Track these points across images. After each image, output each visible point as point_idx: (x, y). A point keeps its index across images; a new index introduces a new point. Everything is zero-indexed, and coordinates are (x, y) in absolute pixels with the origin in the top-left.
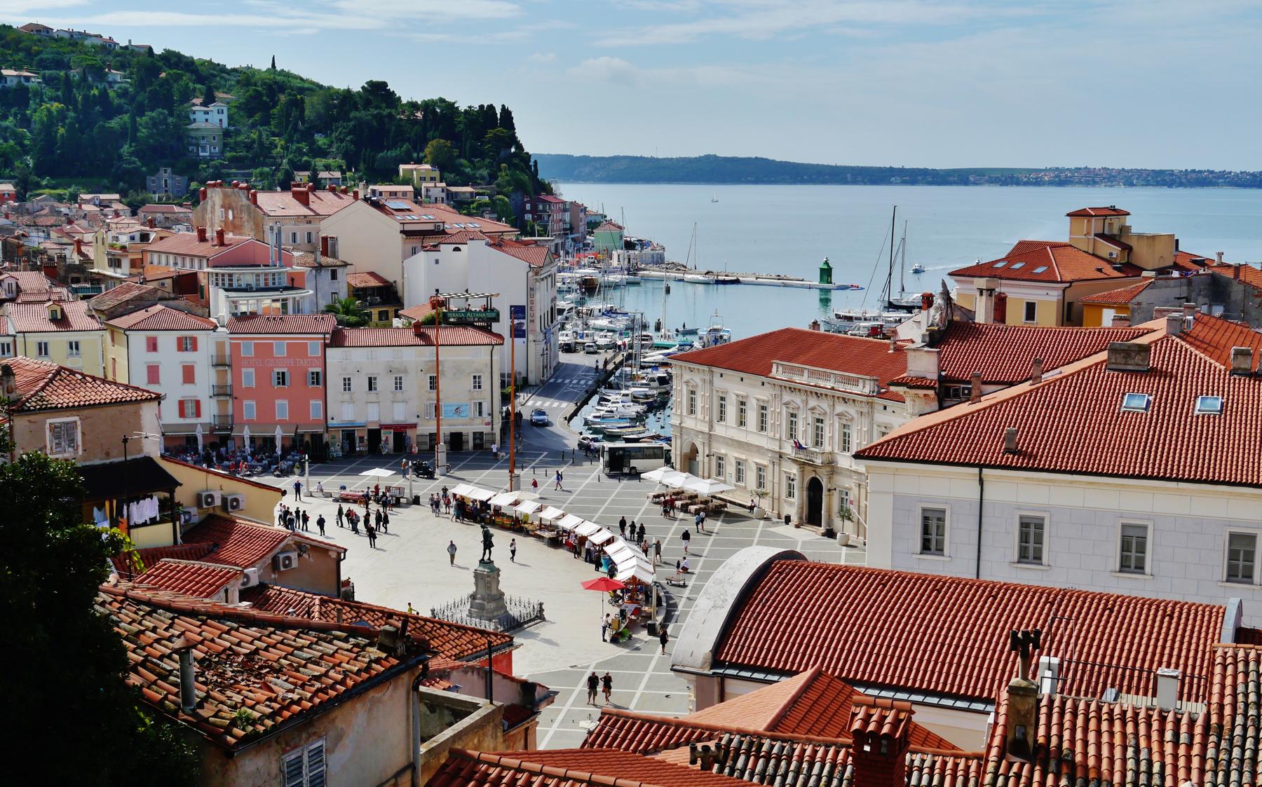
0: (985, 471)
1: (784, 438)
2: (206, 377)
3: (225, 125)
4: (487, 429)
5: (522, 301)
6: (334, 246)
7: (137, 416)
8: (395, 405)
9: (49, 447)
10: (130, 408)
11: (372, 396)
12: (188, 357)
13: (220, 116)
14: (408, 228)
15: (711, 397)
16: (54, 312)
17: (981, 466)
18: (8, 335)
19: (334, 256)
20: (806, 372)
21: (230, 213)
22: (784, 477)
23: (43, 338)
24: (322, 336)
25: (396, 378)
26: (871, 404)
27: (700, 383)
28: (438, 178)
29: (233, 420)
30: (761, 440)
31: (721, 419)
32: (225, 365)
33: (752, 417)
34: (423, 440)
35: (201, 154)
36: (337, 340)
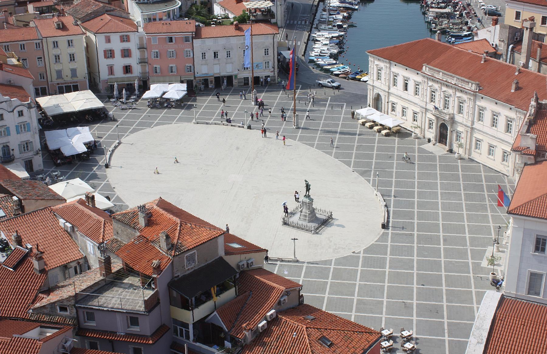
1: (428, 102)
4: (271, 74)
7: (217, 242)
8: (228, 65)
9: (186, 265)
10: (214, 239)
11: (216, 61)
12: (126, 45)
15: (390, 74)
16: (58, 25)
18: (39, 39)
20: (441, 73)
24: (191, 33)
25: (227, 52)
26: (475, 96)
29: (149, 74)
30: (416, 99)
32: (144, 48)
36: (197, 34)
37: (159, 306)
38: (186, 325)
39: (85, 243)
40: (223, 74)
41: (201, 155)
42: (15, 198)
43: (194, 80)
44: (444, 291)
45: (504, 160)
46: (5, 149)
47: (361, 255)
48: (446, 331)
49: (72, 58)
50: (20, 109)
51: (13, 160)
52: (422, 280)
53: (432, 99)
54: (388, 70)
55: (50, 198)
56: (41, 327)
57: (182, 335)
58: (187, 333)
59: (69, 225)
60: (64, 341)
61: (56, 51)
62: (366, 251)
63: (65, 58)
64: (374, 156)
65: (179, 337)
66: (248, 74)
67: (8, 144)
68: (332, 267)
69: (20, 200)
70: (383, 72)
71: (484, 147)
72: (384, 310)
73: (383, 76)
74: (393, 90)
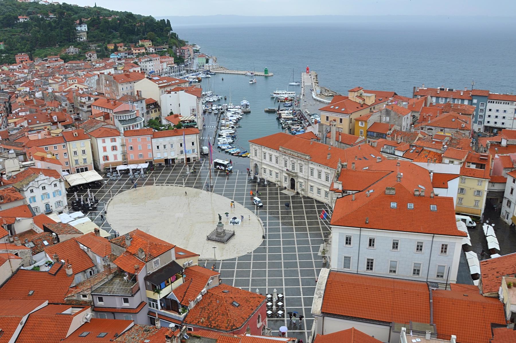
0: (362, 229)
3: (87, 30)
4: (196, 156)
5: (195, 108)
6: (140, 93)
7: (170, 252)
10: (169, 251)
12: (114, 144)
13: (85, 28)
14: (160, 85)
17: (361, 228)
21: (108, 82)
22: (283, 177)
27: (258, 149)
28: (151, 44)
30: (277, 166)
31: (265, 158)
33: (274, 159)
34: (179, 160)
35: (81, 40)
37: (139, 291)
38: (155, 301)
39: (96, 257)
40: (169, 157)
41: (159, 203)
42: (54, 234)
43: (153, 162)
44: (299, 271)
45: (326, 196)
46: (47, 206)
47: (252, 254)
48: (302, 293)
49: (84, 152)
50: (55, 183)
51: (52, 212)
52: (286, 265)
53: (286, 165)
54: (260, 151)
55: (74, 233)
56: (72, 307)
57: (154, 307)
58: (157, 305)
59: (86, 248)
60: (86, 315)
62: (255, 251)
63: (80, 153)
65: (152, 308)
66: (183, 157)
67: (49, 203)
68: (237, 262)
69: (57, 235)
70: (258, 152)
71: (315, 190)
72: (267, 284)
73: (258, 154)
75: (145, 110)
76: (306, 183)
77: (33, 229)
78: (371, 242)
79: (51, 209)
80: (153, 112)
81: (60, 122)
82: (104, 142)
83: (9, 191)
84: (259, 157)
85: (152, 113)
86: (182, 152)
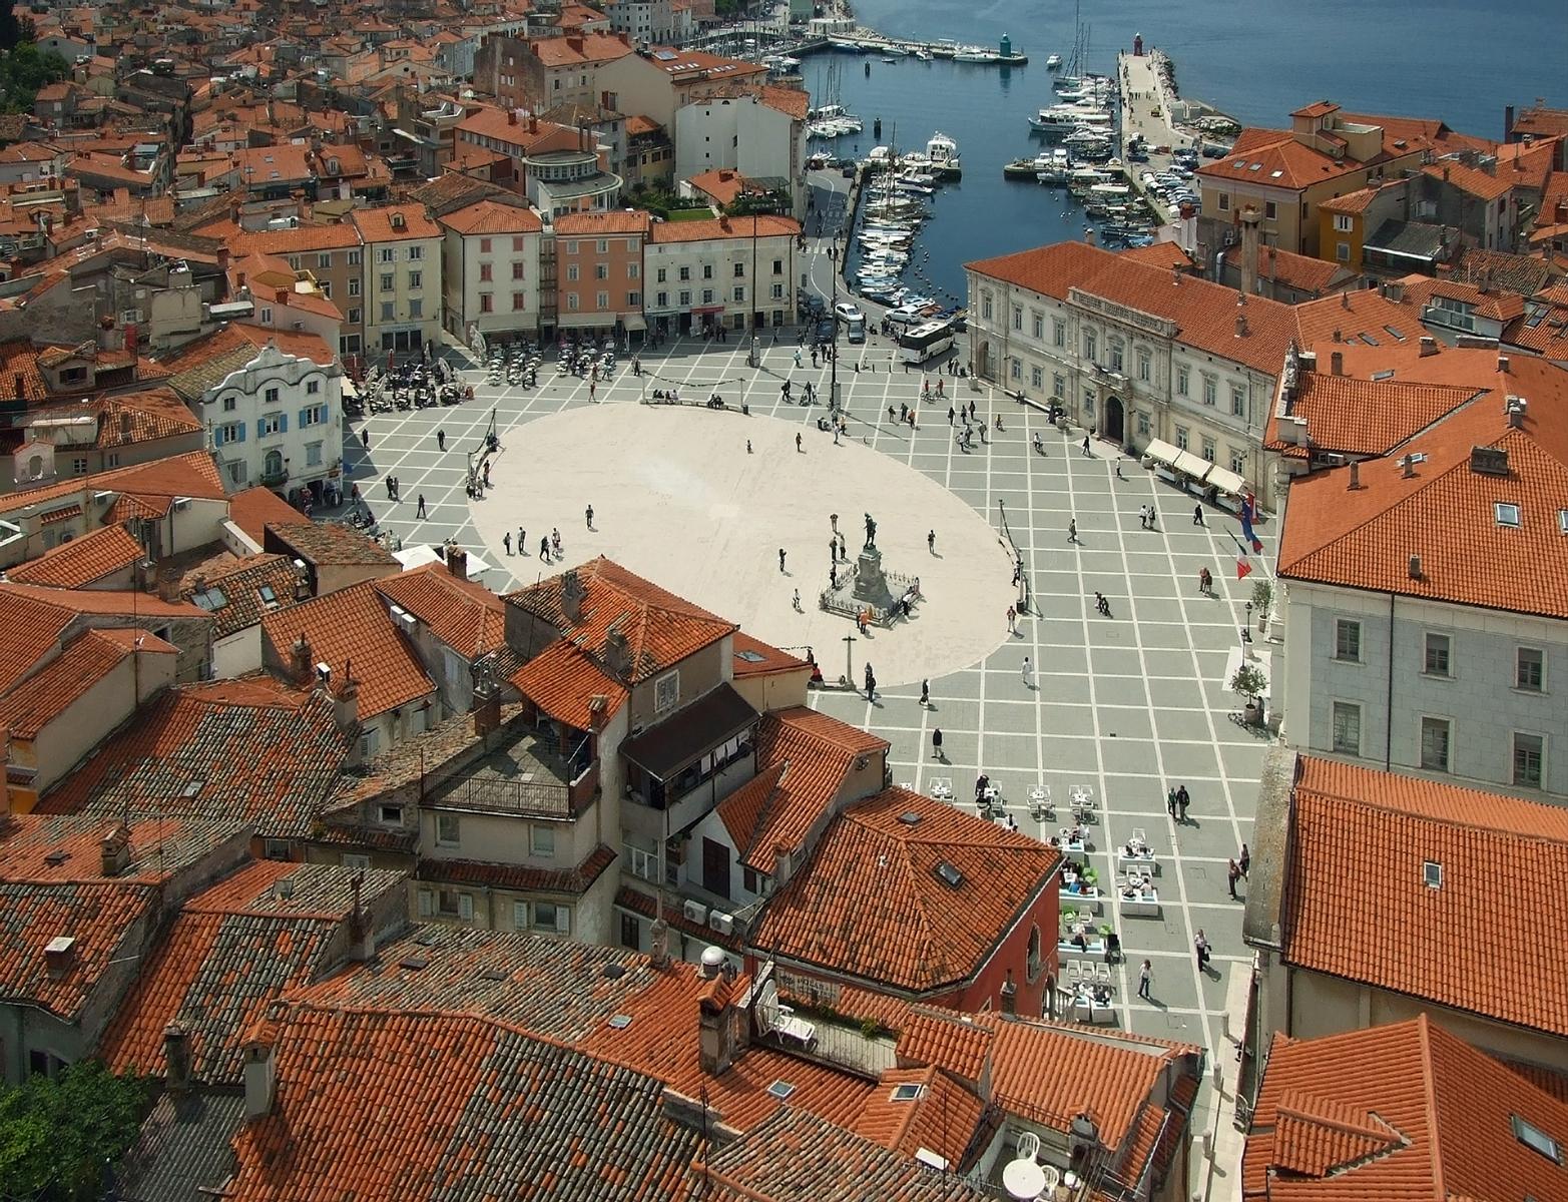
2: (533, 273)
4: (784, 308)
19: (614, 109)
22: (1082, 392)
23: (387, 246)
31: (1018, 326)
47: (983, 671)
50: (311, 378)
53: (1090, 355)
54: (1002, 298)
61: (387, 269)
62: (991, 662)
64: (989, 462)
66: (745, 309)
70: (994, 303)
74: (1014, 334)
75: (624, 153)
76: (1163, 417)
77: (225, 540)
78: (1437, 661)
79: (283, 470)
80: (649, 160)
81: (346, 179)
82: (486, 247)
83: (157, 399)
84: (998, 318)
85: (644, 163)
86: (739, 293)
